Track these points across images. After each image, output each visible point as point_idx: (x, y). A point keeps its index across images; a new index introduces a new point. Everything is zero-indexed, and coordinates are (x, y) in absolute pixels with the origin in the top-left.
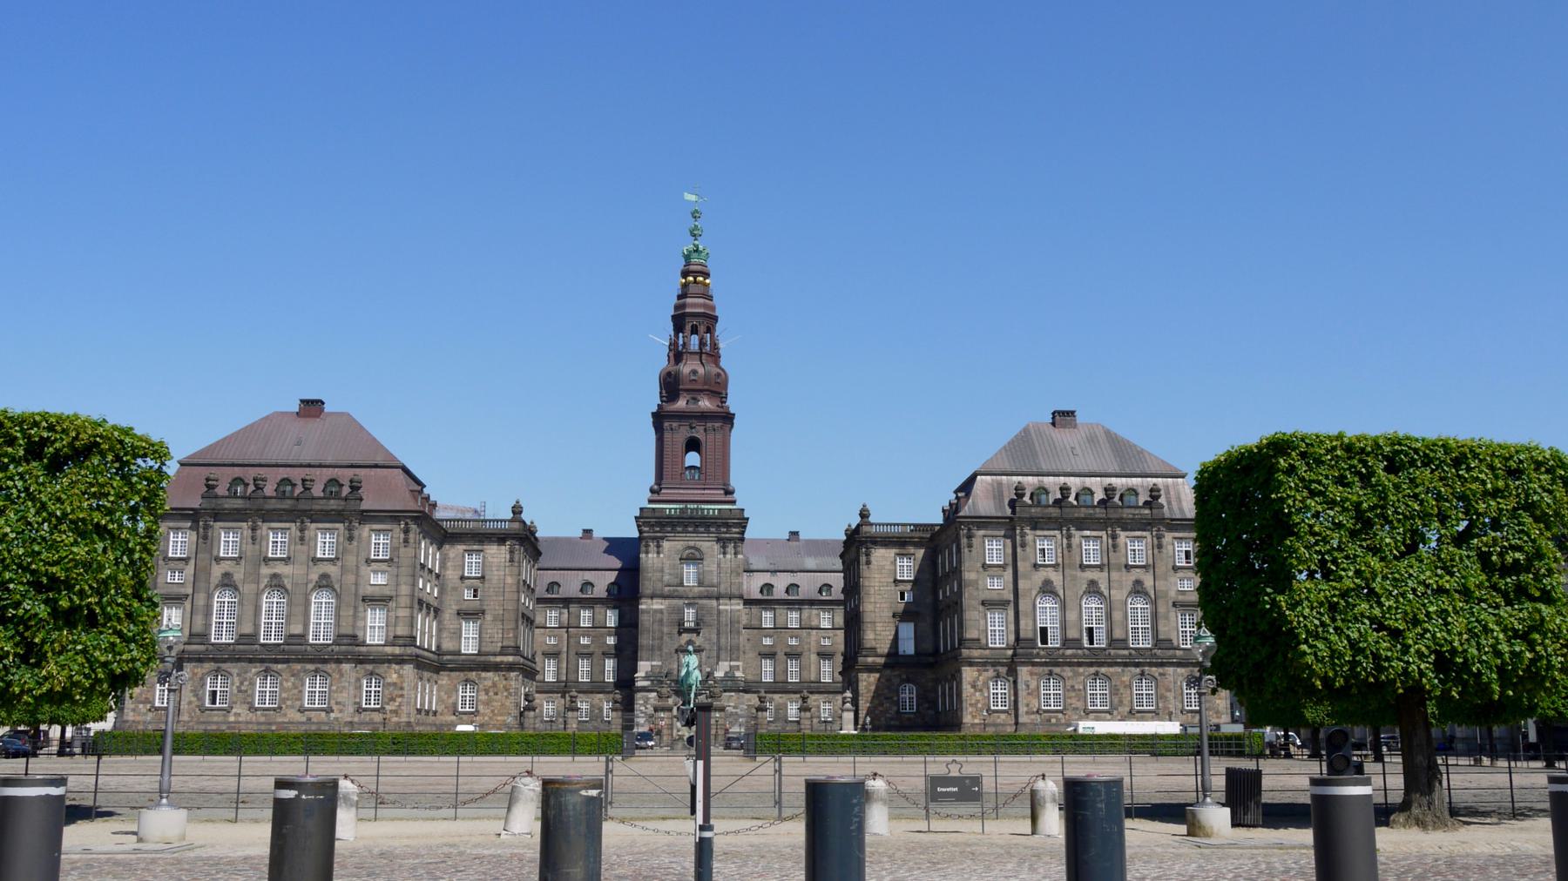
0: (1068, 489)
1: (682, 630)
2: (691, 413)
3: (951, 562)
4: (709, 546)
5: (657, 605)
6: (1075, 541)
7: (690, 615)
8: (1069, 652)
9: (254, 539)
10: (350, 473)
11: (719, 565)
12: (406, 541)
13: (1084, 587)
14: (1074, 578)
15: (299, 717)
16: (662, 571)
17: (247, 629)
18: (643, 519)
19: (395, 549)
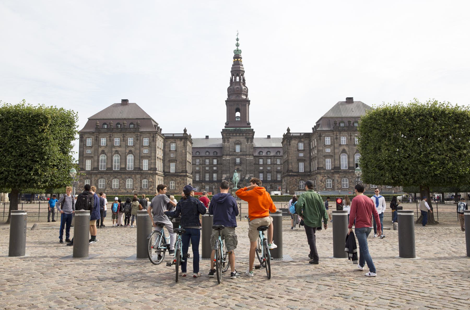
0: (350, 122)
2: (237, 100)
3: (314, 144)
5: (228, 158)
6: (352, 137)
7: (238, 160)
8: (350, 171)
9: (110, 140)
10: (136, 121)
11: (246, 146)
12: (153, 140)
13: (355, 151)
15: (124, 191)
16: (229, 148)
17: (109, 166)
18: (223, 132)
19: (150, 143)
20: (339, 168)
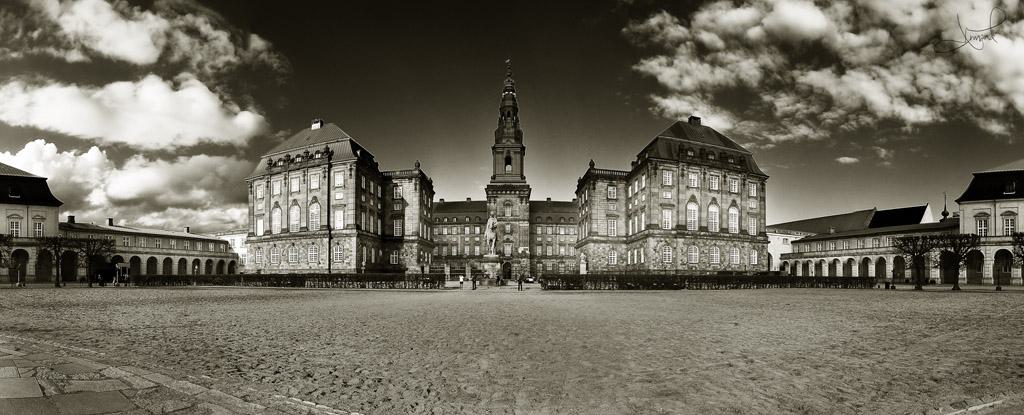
1: (505, 233)
4: (515, 199)
6: (707, 176)
7: (508, 228)
14: (706, 196)
20: (684, 227)
